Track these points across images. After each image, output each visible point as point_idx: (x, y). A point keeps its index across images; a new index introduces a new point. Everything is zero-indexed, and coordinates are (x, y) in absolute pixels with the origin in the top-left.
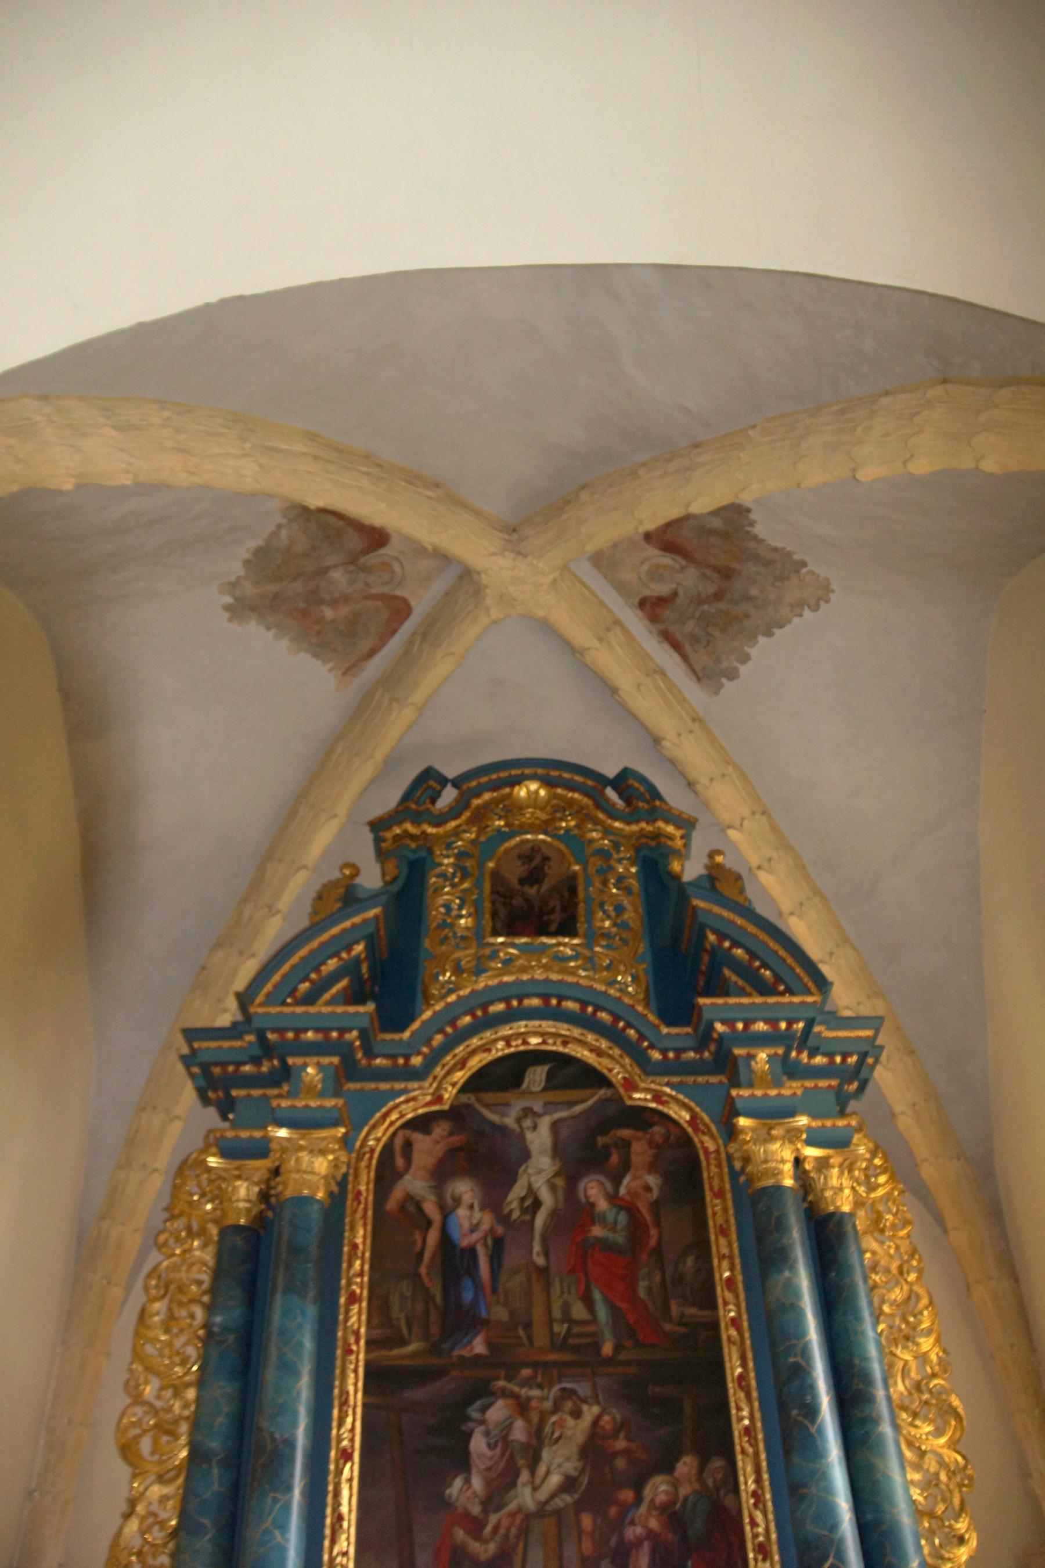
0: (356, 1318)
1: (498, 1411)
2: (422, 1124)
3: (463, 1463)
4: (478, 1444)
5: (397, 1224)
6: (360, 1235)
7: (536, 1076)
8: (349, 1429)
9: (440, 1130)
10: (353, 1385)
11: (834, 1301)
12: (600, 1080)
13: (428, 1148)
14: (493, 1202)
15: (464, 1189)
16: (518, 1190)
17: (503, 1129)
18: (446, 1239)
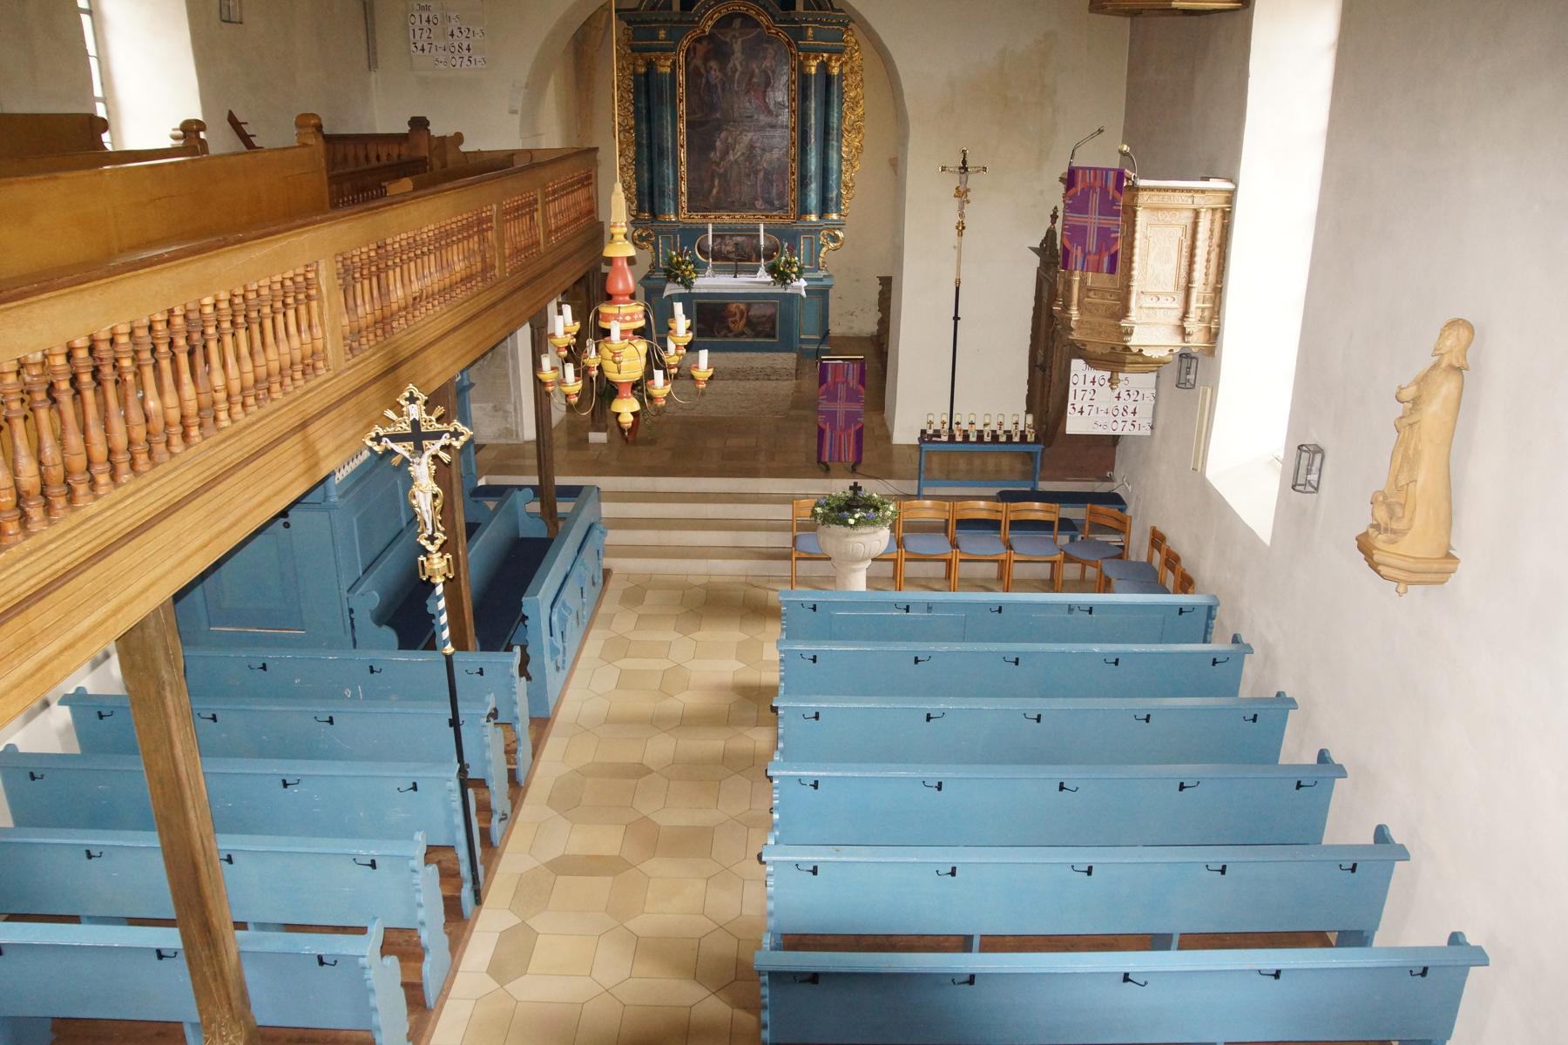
0: (682, 107)
1: (723, 135)
2: (699, 40)
3: (714, 148)
4: (718, 143)
5: (692, 75)
6: (681, 78)
7: (737, 23)
8: (682, 139)
9: (705, 43)
10: (682, 126)
11: (826, 105)
12: (757, 24)
13: (701, 49)
14: (722, 69)
15: (713, 64)
16: (730, 65)
17: (725, 43)
18: (708, 82)
